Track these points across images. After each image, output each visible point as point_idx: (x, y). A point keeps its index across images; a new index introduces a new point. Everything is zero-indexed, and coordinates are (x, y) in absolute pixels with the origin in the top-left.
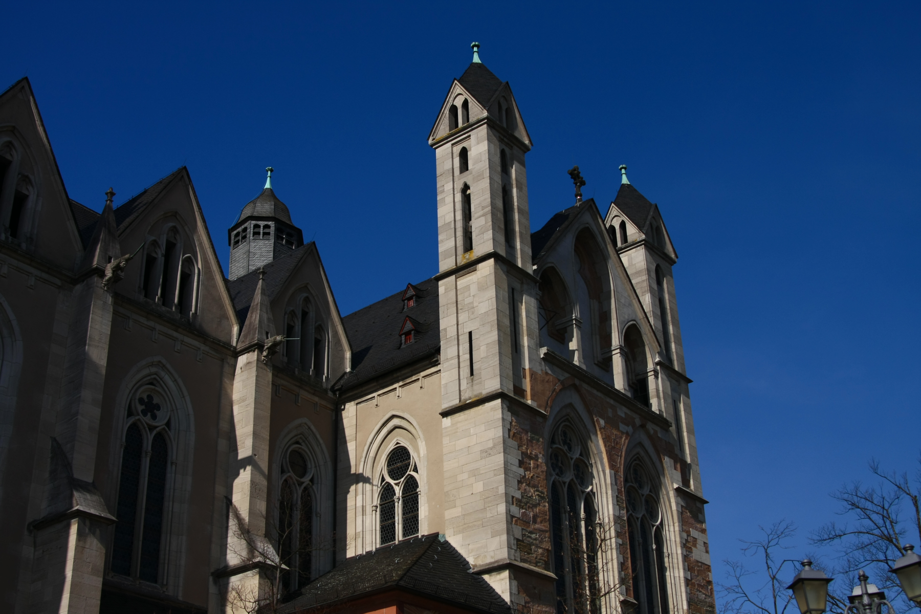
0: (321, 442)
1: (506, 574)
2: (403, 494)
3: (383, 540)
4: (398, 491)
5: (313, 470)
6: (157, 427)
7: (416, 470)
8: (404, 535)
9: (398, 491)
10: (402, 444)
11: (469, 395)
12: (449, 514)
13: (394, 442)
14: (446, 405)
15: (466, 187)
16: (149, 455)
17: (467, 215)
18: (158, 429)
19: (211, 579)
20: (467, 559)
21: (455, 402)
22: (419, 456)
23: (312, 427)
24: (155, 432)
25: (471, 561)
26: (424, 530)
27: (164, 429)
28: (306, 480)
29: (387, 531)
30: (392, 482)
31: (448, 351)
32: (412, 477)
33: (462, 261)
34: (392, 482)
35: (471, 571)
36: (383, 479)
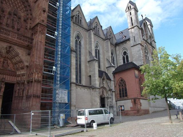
3: (124, 63)
4: (125, 57)
7: (127, 54)
9: (125, 57)
11: (135, 44)
14: (132, 46)
15: (131, 17)
17: (132, 21)
21: (133, 45)
26: (130, 61)
29: (124, 62)
31: (131, 39)
32: (127, 55)
33: (132, 27)
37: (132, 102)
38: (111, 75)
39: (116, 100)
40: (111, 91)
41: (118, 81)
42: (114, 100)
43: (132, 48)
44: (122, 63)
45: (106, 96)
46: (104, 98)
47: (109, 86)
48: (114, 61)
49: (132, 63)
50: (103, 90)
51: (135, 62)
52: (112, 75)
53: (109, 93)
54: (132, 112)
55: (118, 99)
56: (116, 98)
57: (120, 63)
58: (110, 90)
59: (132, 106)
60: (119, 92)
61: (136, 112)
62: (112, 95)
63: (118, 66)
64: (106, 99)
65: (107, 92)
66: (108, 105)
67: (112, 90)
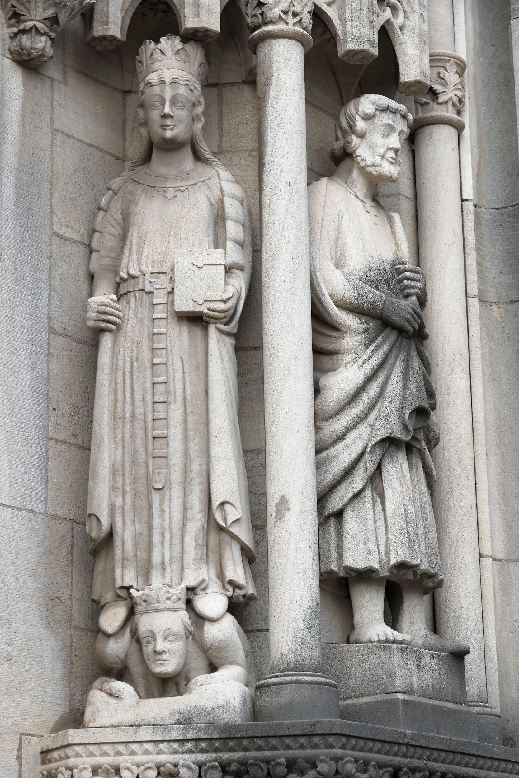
66: (173, 587)
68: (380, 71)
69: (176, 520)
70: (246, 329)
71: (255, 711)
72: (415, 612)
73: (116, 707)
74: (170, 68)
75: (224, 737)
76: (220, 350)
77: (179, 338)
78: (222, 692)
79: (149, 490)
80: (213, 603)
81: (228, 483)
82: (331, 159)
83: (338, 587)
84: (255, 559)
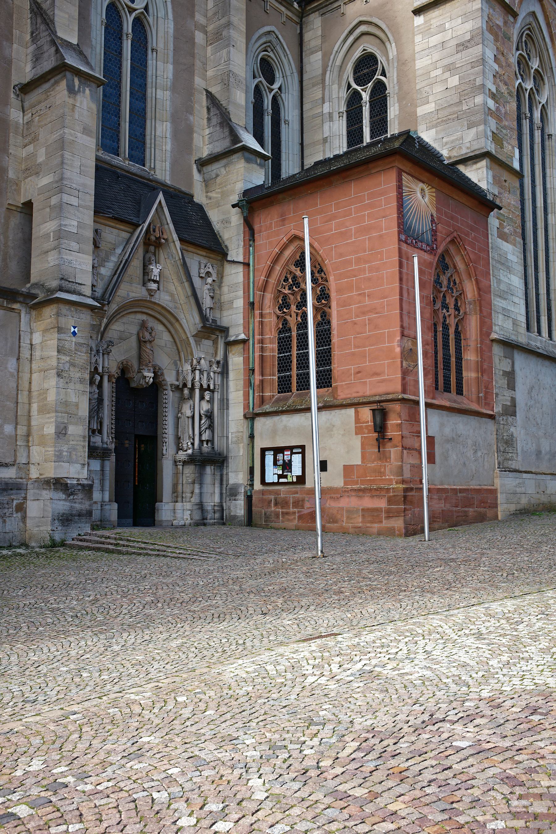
0: (288, 52)
1: (483, 163)
2: (370, 99)
3: (349, 144)
4: (366, 96)
5: (281, 79)
6: (136, 10)
7: (384, 74)
8: (372, 137)
9: (366, 96)
10: (369, 50)
12: (421, 111)
13: (361, 48)
16: (130, 36)
18: (137, 12)
19: (195, 167)
20: (441, 152)
22: (388, 60)
23: (280, 37)
24: (134, 15)
25: (445, 153)
26: (393, 129)
27: (142, 13)
28: (276, 86)
29: (354, 135)
30: (359, 88)
34: (359, 88)
35: (446, 162)
36: (349, 86)
37: (358, 431)
38: (228, 223)
39: (246, 406)
40: (215, 342)
41: (276, 260)
42: (236, 411)
43: (419, 20)
44: (340, 146)
45: (170, 378)
46: (156, 388)
47: (207, 302)
48: (283, 126)
49: (408, 138)
50: (143, 325)
51: (428, 136)
52: (236, 218)
53: (202, 352)
54: (350, 502)
55: (262, 401)
56: (246, 396)
57: (325, 140)
58: (212, 329)
59: (357, 460)
60: (272, 347)
61: (382, 504)
62: (224, 372)
63: (309, 162)
64: (169, 397)
65: (180, 348)
66: (186, 443)
67: (225, 330)
68: (208, 388)
69: (186, 436)
70: (193, 417)
71: (193, 453)
72: (209, 444)
73: (181, 452)
74: (186, 391)
75: (189, 456)
76: (190, 420)
77: (187, 419)
78: (190, 451)
79: (183, 433)
80: (189, 444)
81: (191, 433)
82: (202, 398)
83: (201, 442)
84: (193, 439)
